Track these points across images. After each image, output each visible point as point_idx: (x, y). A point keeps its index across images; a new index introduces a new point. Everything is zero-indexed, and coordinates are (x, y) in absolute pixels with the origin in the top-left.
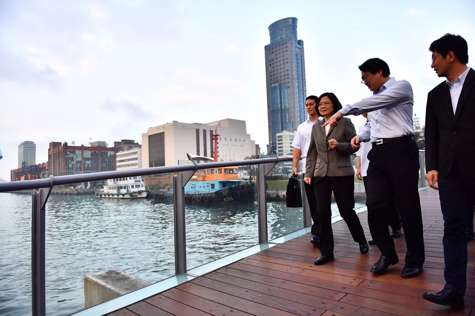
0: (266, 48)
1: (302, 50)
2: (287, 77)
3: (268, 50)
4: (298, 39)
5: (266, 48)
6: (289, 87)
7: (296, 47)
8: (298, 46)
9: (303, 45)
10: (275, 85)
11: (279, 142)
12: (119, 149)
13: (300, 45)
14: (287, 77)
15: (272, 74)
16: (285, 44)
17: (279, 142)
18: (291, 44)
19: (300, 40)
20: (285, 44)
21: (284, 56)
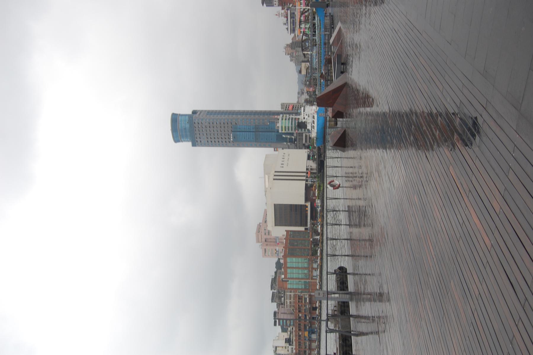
0: (194, 145)
2: (226, 125)
8: (198, 113)
9: (197, 110)
12: (280, 295)
13: (197, 112)
14: (226, 125)
17: (287, 130)
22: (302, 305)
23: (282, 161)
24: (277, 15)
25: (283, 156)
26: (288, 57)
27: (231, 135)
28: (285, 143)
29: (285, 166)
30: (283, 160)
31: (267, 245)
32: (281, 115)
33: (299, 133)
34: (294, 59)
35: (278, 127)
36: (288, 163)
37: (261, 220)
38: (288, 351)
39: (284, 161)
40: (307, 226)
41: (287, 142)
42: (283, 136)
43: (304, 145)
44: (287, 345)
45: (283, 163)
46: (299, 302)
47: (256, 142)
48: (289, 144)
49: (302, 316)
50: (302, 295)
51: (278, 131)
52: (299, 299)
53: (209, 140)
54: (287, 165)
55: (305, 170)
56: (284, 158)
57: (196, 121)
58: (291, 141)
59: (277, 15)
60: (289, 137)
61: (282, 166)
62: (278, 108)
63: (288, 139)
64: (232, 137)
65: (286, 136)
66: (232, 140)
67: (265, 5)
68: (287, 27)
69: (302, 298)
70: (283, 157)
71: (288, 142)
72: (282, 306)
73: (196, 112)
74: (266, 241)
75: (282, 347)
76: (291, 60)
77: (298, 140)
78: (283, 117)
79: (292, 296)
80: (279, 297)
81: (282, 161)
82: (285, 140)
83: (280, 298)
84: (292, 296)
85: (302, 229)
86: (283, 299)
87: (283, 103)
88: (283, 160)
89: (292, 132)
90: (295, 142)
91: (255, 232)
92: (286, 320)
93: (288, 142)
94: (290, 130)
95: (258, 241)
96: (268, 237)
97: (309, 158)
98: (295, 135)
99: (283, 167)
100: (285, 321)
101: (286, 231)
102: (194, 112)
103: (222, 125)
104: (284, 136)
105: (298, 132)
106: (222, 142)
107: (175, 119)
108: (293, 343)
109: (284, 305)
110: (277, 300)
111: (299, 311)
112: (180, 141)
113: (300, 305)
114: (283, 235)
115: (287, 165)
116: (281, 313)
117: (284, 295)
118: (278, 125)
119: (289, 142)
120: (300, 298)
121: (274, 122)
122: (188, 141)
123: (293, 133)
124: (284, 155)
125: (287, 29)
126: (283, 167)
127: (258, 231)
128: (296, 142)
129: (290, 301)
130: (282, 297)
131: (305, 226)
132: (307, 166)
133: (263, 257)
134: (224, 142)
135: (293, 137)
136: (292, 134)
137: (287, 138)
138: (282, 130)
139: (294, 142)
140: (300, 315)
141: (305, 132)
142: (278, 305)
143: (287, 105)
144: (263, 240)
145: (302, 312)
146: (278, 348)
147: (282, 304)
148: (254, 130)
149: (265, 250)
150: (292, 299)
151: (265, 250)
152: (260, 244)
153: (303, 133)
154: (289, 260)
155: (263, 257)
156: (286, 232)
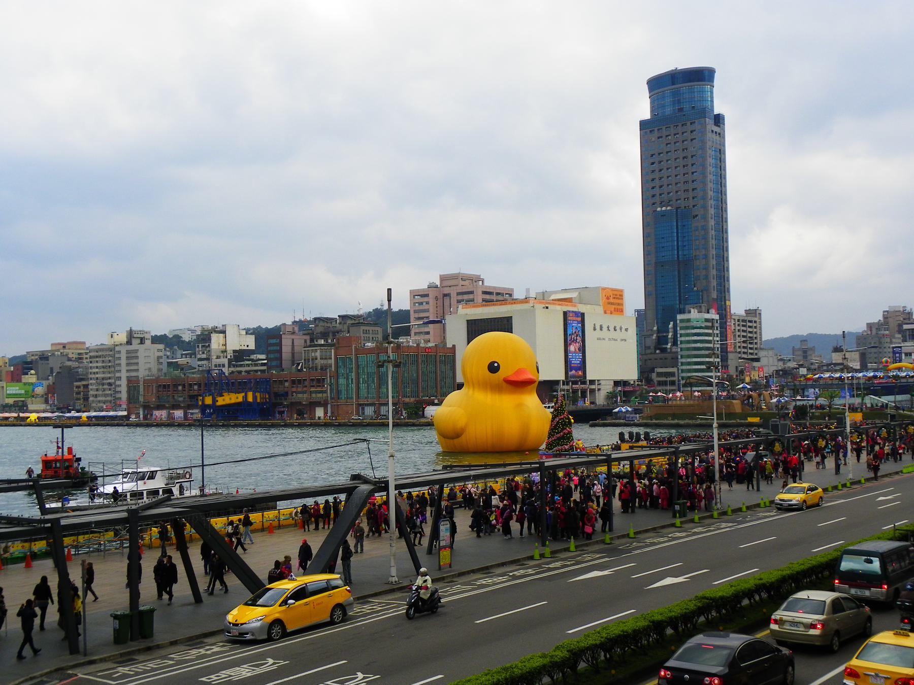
0: (643, 124)
2: (691, 194)
3: (648, 131)
4: (716, 112)
5: (643, 124)
6: (697, 216)
7: (712, 131)
8: (716, 129)
10: (664, 208)
11: (683, 332)
12: (331, 335)
13: (719, 126)
15: (657, 183)
16: (689, 123)
17: (683, 332)
18: (704, 125)
20: (689, 123)
21: (687, 149)
22: (306, 386)
23: (608, 327)
25: (621, 329)
26: (877, 317)
28: (655, 328)
29: (598, 333)
30: (612, 328)
31: (437, 299)
32: (717, 317)
33: (678, 358)
34: (874, 331)
36: (604, 339)
37: (491, 282)
38: (218, 357)
39: (609, 330)
41: (658, 331)
42: (672, 323)
43: (652, 370)
44: (230, 355)
45: (605, 328)
46: (312, 380)
47: (656, 263)
48: (654, 337)
49: (285, 387)
50: (326, 386)
51: (682, 311)
52: (318, 380)
53: (656, 159)
54: (599, 339)
55: (589, 377)
56: (609, 330)
57: (697, 126)
58: (661, 341)
60: (670, 335)
61: (598, 327)
62: (737, 306)
63: (665, 334)
64: (664, 208)
66: (659, 209)
69: (320, 386)
70: (618, 328)
71: (658, 335)
73: (719, 122)
74: (445, 295)
75: (225, 345)
76: (870, 326)
77: (663, 355)
79: (329, 361)
80: (325, 333)
81: (608, 327)
82: (663, 329)
83: (324, 335)
84: (329, 361)
86: (322, 342)
87: (760, 314)
88: (612, 328)
89: (679, 343)
90: (658, 349)
91: (462, 272)
92: (280, 351)
96: (454, 301)
97: (617, 383)
98: (674, 350)
99: (595, 329)
101: (454, 346)
102: (719, 120)
103: (691, 186)
104: (671, 325)
105: (679, 357)
106: (653, 188)
108: (234, 366)
109: (310, 346)
110: (320, 329)
111: (293, 382)
112: (652, 93)
113: (306, 383)
115: (599, 339)
116: (293, 340)
118: (692, 310)
119: (658, 337)
120: (320, 382)
121: (699, 300)
122: (652, 111)
123: (677, 345)
124: (623, 330)
126: (595, 329)
127: (465, 278)
128: (658, 351)
129: (319, 358)
130: (326, 340)
132: (598, 380)
133: (411, 292)
135: (669, 346)
136: (675, 343)
137: (668, 332)
138: (682, 321)
139: (659, 346)
140: (287, 384)
141: (680, 371)
142: (311, 332)
143: (755, 322)
144: (446, 291)
145: (293, 387)
146: (222, 335)
147: (312, 340)
149: (427, 295)
150: (323, 362)
151: (427, 295)
152: (438, 283)
153: (677, 366)
155: (411, 292)
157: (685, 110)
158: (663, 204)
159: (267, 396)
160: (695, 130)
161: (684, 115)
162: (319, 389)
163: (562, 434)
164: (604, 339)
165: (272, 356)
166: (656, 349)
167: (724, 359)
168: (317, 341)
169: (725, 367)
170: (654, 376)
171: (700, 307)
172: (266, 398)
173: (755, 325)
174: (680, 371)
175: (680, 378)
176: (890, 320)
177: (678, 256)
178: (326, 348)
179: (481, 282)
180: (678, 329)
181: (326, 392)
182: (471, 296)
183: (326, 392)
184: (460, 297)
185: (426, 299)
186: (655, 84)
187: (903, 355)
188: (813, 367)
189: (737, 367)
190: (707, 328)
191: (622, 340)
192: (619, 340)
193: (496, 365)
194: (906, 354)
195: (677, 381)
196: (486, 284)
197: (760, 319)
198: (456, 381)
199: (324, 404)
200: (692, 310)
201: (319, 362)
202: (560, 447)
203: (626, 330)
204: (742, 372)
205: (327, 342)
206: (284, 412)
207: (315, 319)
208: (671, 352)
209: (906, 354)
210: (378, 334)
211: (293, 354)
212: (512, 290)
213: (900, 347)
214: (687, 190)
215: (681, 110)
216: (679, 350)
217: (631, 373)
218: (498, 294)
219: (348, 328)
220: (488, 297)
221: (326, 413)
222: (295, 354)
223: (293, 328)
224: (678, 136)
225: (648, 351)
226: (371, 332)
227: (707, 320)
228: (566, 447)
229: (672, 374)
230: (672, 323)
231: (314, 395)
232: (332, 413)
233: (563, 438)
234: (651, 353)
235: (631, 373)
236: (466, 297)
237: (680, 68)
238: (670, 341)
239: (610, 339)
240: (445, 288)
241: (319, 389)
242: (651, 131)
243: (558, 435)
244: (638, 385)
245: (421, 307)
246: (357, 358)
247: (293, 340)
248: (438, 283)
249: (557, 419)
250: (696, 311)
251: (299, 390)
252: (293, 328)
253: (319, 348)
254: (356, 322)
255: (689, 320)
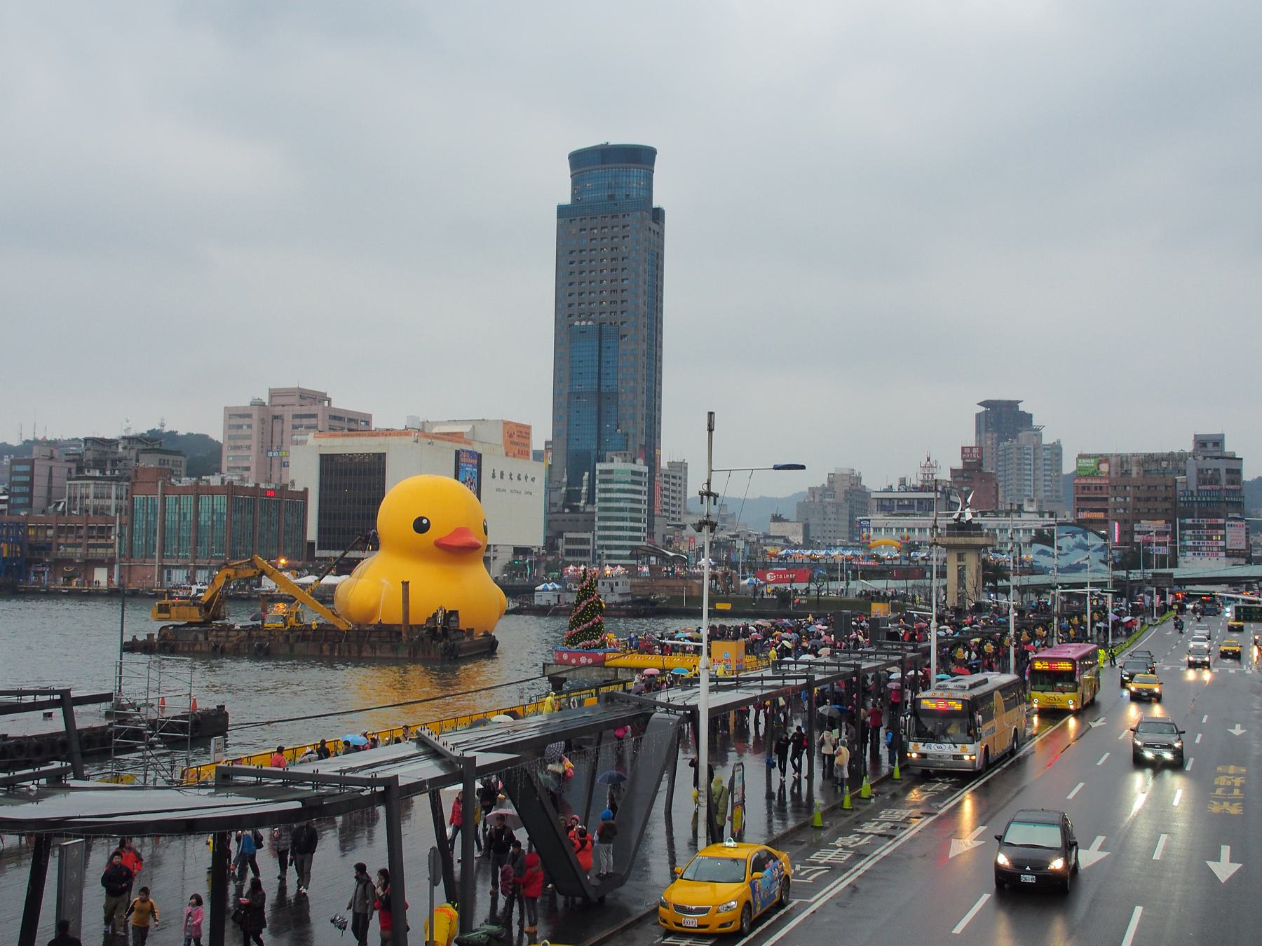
0: (562, 211)
1: (660, 235)
3: (568, 220)
4: (655, 204)
5: (562, 211)
7: (650, 229)
8: (654, 226)
10: (583, 323)
12: (109, 465)
13: (658, 224)
15: (576, 288)
19: (659, 208)
21: (616, 249)
22: (81, 537)
23: (511, 475)
24: (928, 460)
25: (526, 477)
27: (590, 323)
28: (565, 479)
29: (498, 482)
30: (515, 477)
31: (263, 421)
32: (645, 469)
33: (594, 520)
34: (817, 497)
35: (612, 461)
36: (504, 491)
37: (342, 401)
40: (318, 549)
41: (568, 484)
42: (587, 474)
43: (560, 535)
45: (506, 477)
47: (570, 394)
48: (564, 489)
49: (46, 537)
50: (113, 537)
51: (601, 459)
52: (101, 529)
58: (572, 497)
59: (928, 460)
60: (584, 489)
61: (498, 475)
65: (585, 483)
66: (577, 323)
67: (982, 409)
68: (895, 488)
69: (103, 537)
70: (522, 477)
72: (74, 471)
73: (658, 218)
74: (276, 417)
76: (813, 491)
77: (573, 516)
78: (640, 474)
79: (108, 502)
81: (511, 475)
82: (575, 480)
83: (99, 464)
84: (108, 502)
85: (312, 534)
86: (97, 473)
87: (686, 468)
88: (515, 477)
89: (597, 500)
90: (568, 507)
91: (300, 387)
92: (31, 484)
93: (567, 486)
94: (603, 495)
95: (274, 394)
97: (518, 551)
98: (588, 509)
99: (494, 476)
100: (27, 478)
101: (306, 490)
102: (658, 215)
105: (596, 519)
106: (570, 295)
107: (641, 158)
110: (90, 455)
111: (60, 529)
112: (575, 171)
113: (82, 532)
114: (293, 483)
116: (51, 468)
117: (112, 479)
120: (104, 531)
121: (623, 448)
122: (573, 195)
123: (594, 503)
124: (529, 479)
125: (890, 489)
126: (494, 476)
128: (567, 510)
129: (91, 496)
130: (103, 471)
131: (319, 544)
132: (494, 546)
134: (570, 300)
135: (582, 503)
136: (591, 500)
138: (601, 472)
140: (50, 532)
141: (596, 538)
142: (77, 457)
144: (277, 411)
145: (59, 537)
147: (80, 469)
148: (602, 388)
149: (249, 416)
150: (97, 502)
151: (249, 416)
152: (266, 400)
154: (221, 501)
156: (302, 490)
157: (616, 197)
158: (583, 316)
159: (18, 549)
160: (628, 226)
161: (616, 204)
162: (101, 541)
163: (591, 623)
164: (504, 491)
165: (17, 490)
166: (564, 506)
167: (651, 525)
168: (88, 471)
169: (651, 534)
170: (561, 542)
171: (625, 455)
172: (16, 552)
173: (679, 482)
174: (596, 538)
175: (596, 547)
176: (836, 485)
177: (599, 385)
178: (103, 482)
179: (326, 403)
180: (597, 482)
181: (112, 546)
182: (313, 421)
183: (112, 546)
184: (297, 422)
185: (247, 421)
186: (580, 160)
187: (872, 530)
188: (751, 540)
189: (664, 536)
190: (633, 482)
191: (527, 493)
192: (523, 493)
193: (425, 521)
194: (875, 529)
195: (591, 552)
196: (333, 406)
197: (686, 474)
198: (306, 538)
199: (108, 564)
200: (615, 458)
201: (91, 502)
202: (588, 642)
203: (533, 479)
204: (670, 542)
205: (105, 474)
206: (43, 573)
207: (86, 440)
208: (584, 512)
209: (875, 529)
210: (181, 466)
211: (50, 489)
212: (370, 416)
213: (869, 520)
214: (615, 302)
215: (611, 197)
216: (596, 510)
217: (535, 538)
218: (350, 420)
219: (137, 455)
220: (336, 423)
221: (110, 577)
222: (53, 489)
223: (52, 451)
224: (606, 230)
225: (553, 509)
226: (171, 463)
227: (634, 473)
228: (597, 642)
229: (586, 541)
230: (587, 474)
231: (91, 550)
232: (121, 577)
233: (592, 629)
234: (558, 512)
235: (535, 538)
236: (305, 422)
237: (612, 143)
238: (583, 496)
239: (511, 491)
240: (277, 408)
241: (101, 541)
242: (571, 221)
243: (586, 625)
244: (543, 554)
245: (240, 432)
246: (164, 500)
247: (51, 468)
248: (266, 400)
249: (585, 603)
250: (620, 460)
251: (69, 541)
252: (52, 451)
253: (93, 482)
254: (149, 447)
255: (610, 472)
